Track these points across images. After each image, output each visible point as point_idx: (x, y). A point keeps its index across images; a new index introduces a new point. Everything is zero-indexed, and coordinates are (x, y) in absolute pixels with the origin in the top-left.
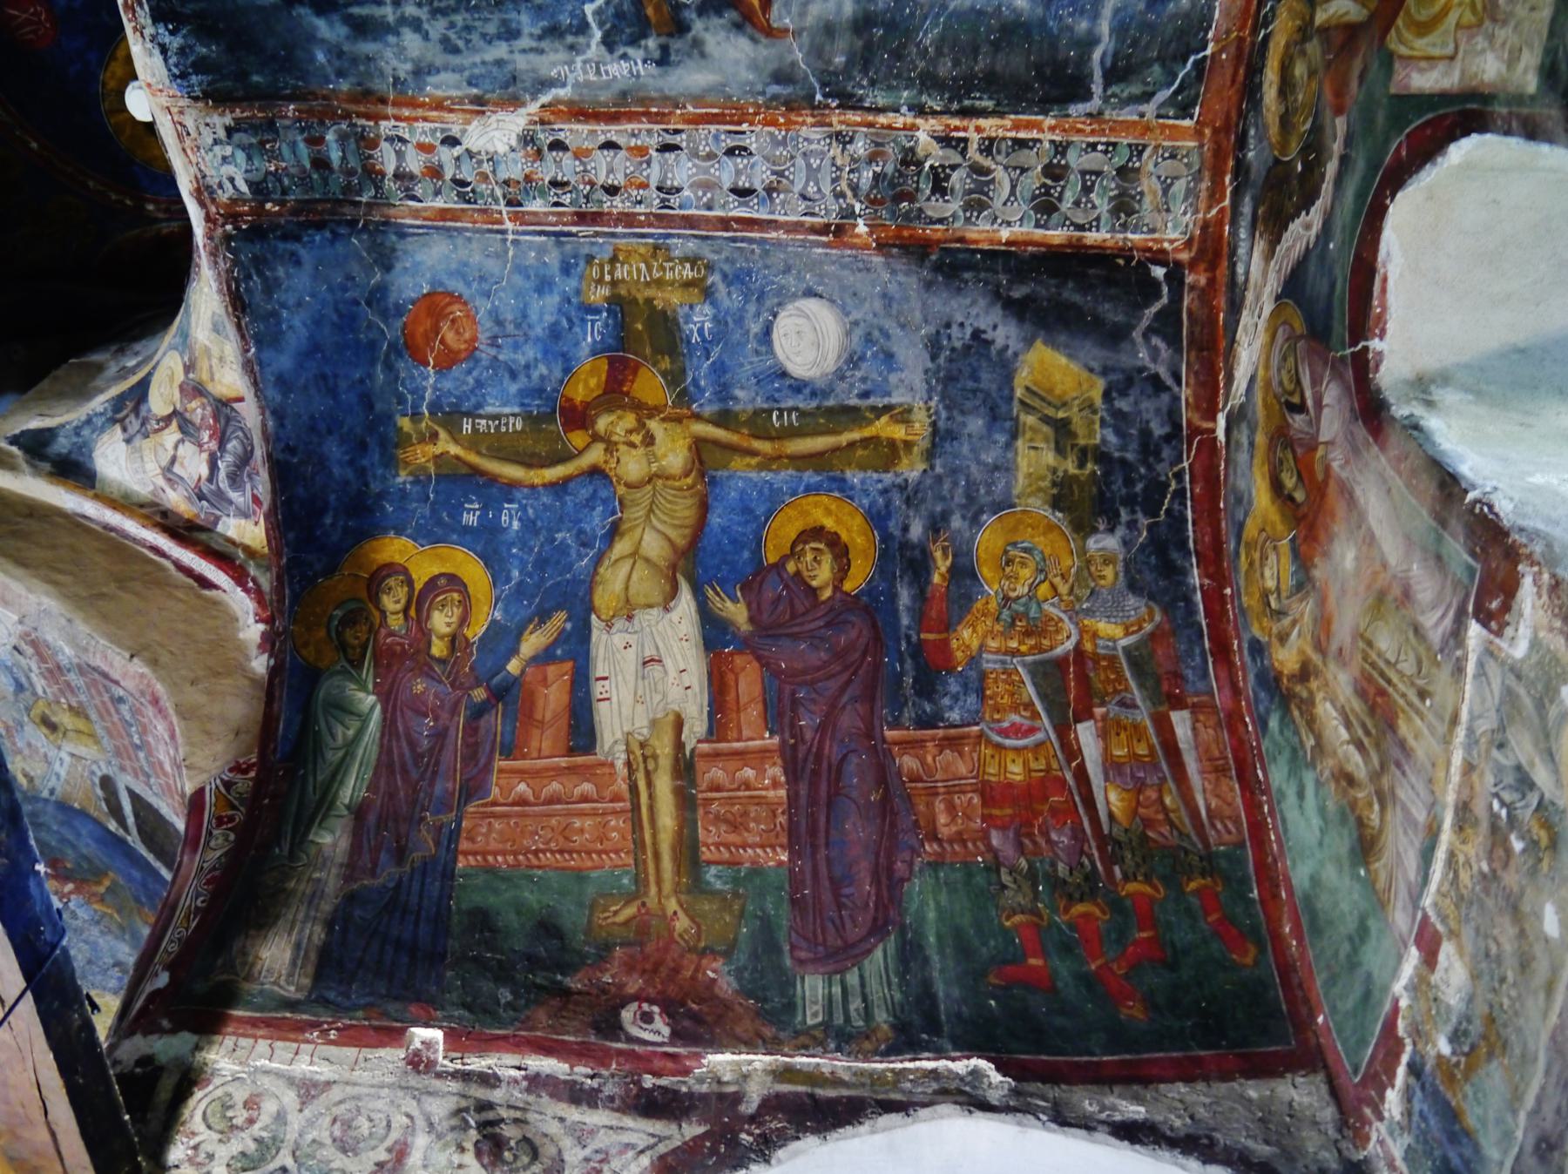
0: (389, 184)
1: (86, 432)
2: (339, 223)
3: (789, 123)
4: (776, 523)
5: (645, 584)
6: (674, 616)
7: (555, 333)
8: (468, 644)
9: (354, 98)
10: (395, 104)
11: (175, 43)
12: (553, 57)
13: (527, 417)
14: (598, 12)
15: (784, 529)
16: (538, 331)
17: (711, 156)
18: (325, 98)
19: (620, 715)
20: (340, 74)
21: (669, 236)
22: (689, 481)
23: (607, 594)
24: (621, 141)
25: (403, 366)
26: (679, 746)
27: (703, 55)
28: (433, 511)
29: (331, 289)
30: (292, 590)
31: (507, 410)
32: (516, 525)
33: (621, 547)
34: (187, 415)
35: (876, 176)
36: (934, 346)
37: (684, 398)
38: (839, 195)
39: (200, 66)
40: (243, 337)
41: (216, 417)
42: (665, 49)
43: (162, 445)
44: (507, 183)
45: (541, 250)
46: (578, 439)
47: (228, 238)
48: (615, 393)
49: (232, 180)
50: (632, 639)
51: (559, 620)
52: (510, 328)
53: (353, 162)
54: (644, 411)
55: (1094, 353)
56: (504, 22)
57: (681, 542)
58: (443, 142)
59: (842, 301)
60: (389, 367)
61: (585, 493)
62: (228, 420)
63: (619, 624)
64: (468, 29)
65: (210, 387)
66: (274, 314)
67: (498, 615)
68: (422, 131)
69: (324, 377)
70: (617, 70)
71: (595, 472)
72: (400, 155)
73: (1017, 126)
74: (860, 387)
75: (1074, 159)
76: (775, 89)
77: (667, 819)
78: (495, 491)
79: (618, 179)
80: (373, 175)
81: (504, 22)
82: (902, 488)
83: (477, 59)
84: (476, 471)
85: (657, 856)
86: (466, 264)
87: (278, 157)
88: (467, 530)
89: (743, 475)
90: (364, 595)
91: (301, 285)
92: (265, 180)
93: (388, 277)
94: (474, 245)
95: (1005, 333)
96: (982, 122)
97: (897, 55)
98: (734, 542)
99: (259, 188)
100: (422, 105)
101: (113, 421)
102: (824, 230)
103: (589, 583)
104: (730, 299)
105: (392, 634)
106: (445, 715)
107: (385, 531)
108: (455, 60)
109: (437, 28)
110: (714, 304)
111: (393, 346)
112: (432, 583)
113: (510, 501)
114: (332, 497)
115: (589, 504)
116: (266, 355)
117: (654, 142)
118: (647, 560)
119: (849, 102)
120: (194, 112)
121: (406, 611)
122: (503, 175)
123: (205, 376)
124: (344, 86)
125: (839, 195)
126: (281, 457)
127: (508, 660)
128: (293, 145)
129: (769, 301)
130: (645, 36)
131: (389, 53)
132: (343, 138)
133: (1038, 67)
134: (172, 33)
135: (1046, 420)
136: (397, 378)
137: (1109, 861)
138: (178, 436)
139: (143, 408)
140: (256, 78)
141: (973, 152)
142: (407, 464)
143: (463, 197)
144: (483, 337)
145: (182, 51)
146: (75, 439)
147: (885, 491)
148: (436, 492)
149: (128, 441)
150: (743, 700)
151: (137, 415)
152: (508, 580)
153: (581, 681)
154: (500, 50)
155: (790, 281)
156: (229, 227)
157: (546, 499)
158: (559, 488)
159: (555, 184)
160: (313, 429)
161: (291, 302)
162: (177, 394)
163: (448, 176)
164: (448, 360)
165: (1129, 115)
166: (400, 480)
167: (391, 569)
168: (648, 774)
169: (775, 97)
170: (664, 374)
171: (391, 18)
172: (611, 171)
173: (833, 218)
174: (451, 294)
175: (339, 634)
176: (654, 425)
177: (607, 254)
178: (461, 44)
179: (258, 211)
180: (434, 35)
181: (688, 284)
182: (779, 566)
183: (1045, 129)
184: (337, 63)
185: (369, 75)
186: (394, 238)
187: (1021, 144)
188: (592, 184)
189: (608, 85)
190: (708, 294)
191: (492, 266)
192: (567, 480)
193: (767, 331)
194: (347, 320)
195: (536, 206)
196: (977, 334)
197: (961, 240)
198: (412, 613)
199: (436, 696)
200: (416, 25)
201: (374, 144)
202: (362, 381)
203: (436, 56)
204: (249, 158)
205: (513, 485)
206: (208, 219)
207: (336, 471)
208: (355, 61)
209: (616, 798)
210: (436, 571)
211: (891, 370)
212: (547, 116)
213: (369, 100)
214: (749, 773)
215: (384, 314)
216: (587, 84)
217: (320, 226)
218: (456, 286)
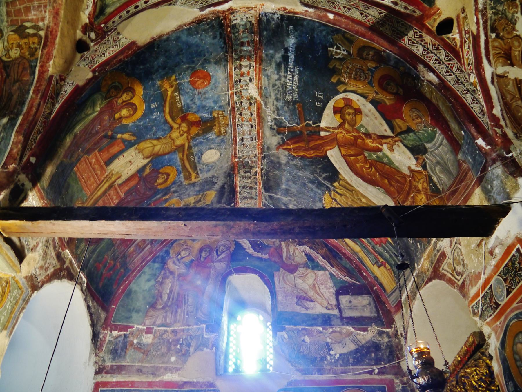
0: (238, 63)
2: (226, 48)
3: (259, 148)
4: (169, 167)
5: (147, 152)
6: (143, 161)
7: (204, 107)
8: (121, 122)
9: (261, 57)
10: (259, 68)
11: (275, 17)
12: (272, 108)
13: (182, 107)
14: (282, 119)
15: (167, 169)
16: (204, 103)
17: (250, 134)
18: (260, 49)
19: (116, 166)
20: (267, 55)
21: (231, 126)
22: (174, 147)
23: (143, 145)
24: (253, 117)
25: (189, 72)
26: (115, 181)
27: (273, 136)
28: (152, 95)
29: (207, 48)
30: (118, 67)
31: (182, 102)
32: (154, 117)
33: (155, 142)
35: (248, 162)
36: (213, 177)
37: (193, 138)
38: (243, 156)
39: (268, 20)
40: (189, 24)
42: (274, 129)
44: (241, 92)
45: (225, 100)
46: (179, 121)
47: (219, 17)
48: (191, 124)
49: (236, 19)
50: (134, 156)
51: (134, 138)
52: (204, 96)
53: (243, 53)
54: (188, 132)
55: (215, 200)
56: (280, 99)
57: (160, 153)
58: (250, 78)
59: (220, 160)
60: (188, 68)
61: (166, 128)
63: (137, 151)
64: (278, 91)
66: (198, 33)
67: (130, 125)
68: (253, 73)
69: (182, 51)
70: (269, 119)
71: (171, 128)
72: (246, 66)
73: (259, 182)
74: (202, 168)
75: (253, 191)
76: (266, 147)
77: (99, 193)
78: (161, 109)
79: (243, 116)
80: (240, 58)
81: (280, 99)
82: (181, 183)
83: (271, 91)
84: (165, 101)
85: (92, 198)
86: (219, 83)
87: (244, 32)
88: (150, 106)
89: (177, 157)
90: (124, 88)
91: (207, 40)
92: (236, 28)
93: (213, 64)
94: (224, 85)
95: (217, 187)
96: (260, 178)
97: (273, 168)
98: (162, 162)
99: (234, 26)
100: (259, 74)
102: (235, 153)
103: (145, 140)
104: (218, 140)
105: (116, 102)
106: (102, 130)
107: (143, 85)
108: (271, 86)
109: (278, 83)
110: (216, 138)
111: (194, 68)
112: (133, 104)
113: (160, 113)
114: (148, 65)
115: (164, 130)
116: (185, 31)
117: (253, 123)
118: (154, 149)
119: (263, 158)
120: (256, 14)
121: (124, 102)
122: (243, 91)
124: (264, 55)
125: (243, 156)
126: (156, 44)
127: (120, 134)
128: (247, 37)
129: (218, 147)
130: (277, 126)
131: (272, 70)
132: (250, 51)
133: (271, 187)
134: (278, 18)
135: (201, 198)
136: (185, 71)
137: (121, 258)
140: (265, 33)
141: (254, 177)
142: (163, 83)
143: (236, 82)
144: (200, 90)
145: (272, 18)
147: (180, 181)
148: (157, 94)
150: (129, 185)
152: (140, 122)
153: (121, 152)
154: (273, 97)
155: (223, 150)
156: (222, 17)
157: (162, 121)
158: (166, 122)
159: (241, 102)
160: (166, 51)
161: (202, 37)
163: (241, 78)
164: (192, 83)
165: (263, 197)
166: (158, 82)
167: (133, 91)
168: (107, 181)
169: (264, 146)
170: (198, 133)
171: (281, 74)
172: (245, 114)
173: (238, 155)
174: (210, 80)
175: (111, 88)
176: (185, 135)
177: (225, 114)
178: (275, 88)
179: (228, 26)
180: (277, 83)
181: (220, 132)
182: (159, 173)
183: (259, 186)
184: (270, 55)
185: (267, 63)
186: (224, 64)
187: (256, 183)
188: (242, 110)
189: (266, 116)
190: (218, 136)
191: (219, 89)
192: (168, 123)
193: (211, 149)
194: (199, 54)
195: (236, 98)
196: (216, 183)
197: (236, 176)
198: (124, 104)
199: (106, 124)
200: (279, 79)
201: (249, 60)
202: (183, 62)
203: (272, 82)
204: (243, 25)
205: (164, 112)
206: (224, 12)
207: (156, 63)
208: (270, 60)
209: (99, 180)
210: (137, 104)
211: (206, 172)
212: (258, 102)
213: (260, 61)
214: (115, 197)
215: (202, 64)
216: (266, 112)
217: (225, 43)
218: (213, 81)
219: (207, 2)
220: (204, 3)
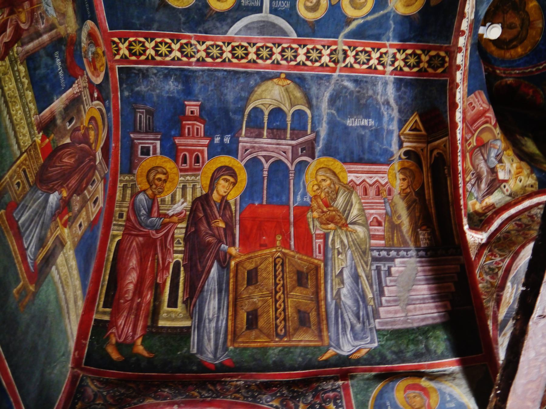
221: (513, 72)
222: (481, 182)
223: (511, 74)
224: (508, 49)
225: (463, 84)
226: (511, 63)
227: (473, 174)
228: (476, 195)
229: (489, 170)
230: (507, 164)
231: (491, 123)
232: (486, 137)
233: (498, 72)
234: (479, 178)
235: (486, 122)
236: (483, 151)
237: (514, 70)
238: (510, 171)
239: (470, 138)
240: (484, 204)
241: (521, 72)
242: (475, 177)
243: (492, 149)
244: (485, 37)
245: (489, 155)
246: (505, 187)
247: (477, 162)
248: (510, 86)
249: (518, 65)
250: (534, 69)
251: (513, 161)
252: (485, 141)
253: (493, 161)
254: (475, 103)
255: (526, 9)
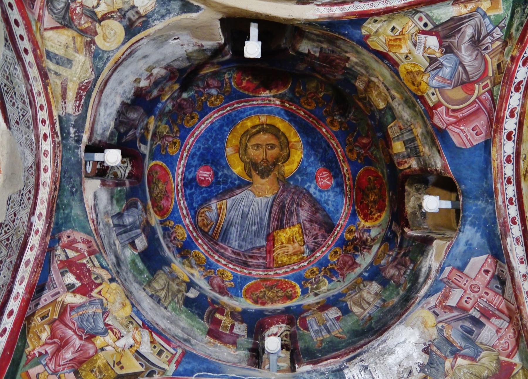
1: (163, 11)
34: (90, 20)
41: (72, 19)
43: (108, 5)
62: (64, 18)
65: (75, 34)
101: (145, 16)
123: (79, 39)
138: (96, 10)
139: (126, 22)
146: (169, 8)
149: (133, 7)
151: (130, 19)
162: (99, 30)
219: (7, 93)
220: (5, 89)
221: (260, 102)
222: (473, 36)
223: (262, 100)
224: (262, 124)
225: (501, 162)
226: (260, 110)
227: (487, 49)
228: (487, 20)
229: (455, 51)
230: (421, 54)
231: (447, 109)
232: (459, 93)
233: (278, 102)
234: (476, 42)
235: (454, 111)
236: (464, 76)
237: (257, 104)
238: (415, 45)
239: (484, 93)
240: (471, 6)
241: (251, 103)
242: (483, 44)
243: (448, 77)
244: (438, 197)
245: (454, 70)
246: (426, 25)
247: (476, 64)
248: (267, 87)
249: (251, 109)
250: (236, 106)
251: (407, 56)
252: (460, 88)
253: (448, 64)
254: (471, 134)
255: (243, 164)
